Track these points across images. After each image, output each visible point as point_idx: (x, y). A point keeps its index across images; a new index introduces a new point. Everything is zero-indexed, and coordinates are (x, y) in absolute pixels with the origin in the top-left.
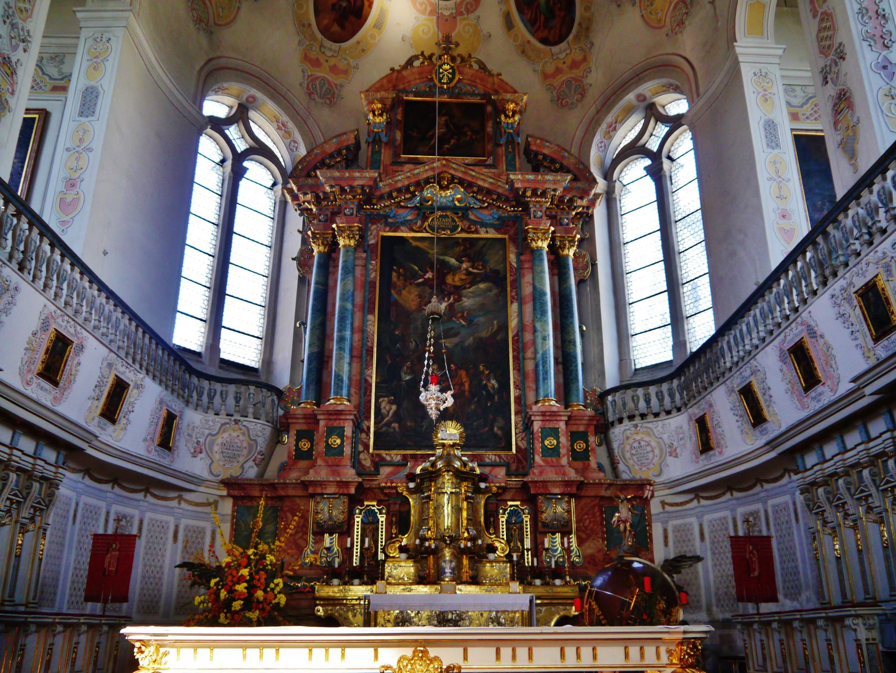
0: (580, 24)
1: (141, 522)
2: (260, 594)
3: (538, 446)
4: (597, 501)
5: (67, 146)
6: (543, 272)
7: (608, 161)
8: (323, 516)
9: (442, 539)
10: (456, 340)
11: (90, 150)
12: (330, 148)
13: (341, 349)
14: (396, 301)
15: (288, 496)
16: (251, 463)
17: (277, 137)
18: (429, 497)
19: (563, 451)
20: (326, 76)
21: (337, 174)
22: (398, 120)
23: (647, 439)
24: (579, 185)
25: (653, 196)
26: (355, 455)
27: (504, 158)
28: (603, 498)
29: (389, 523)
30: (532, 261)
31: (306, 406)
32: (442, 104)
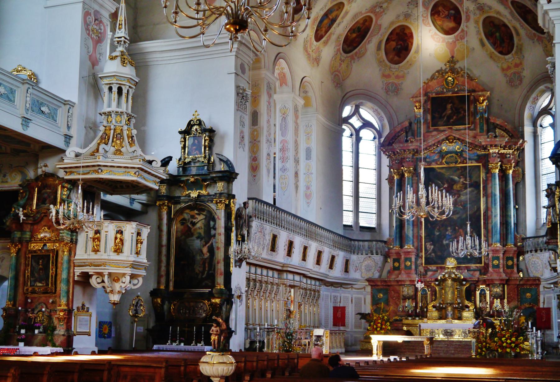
0: (517, 46)
1: (340, 297)
2: (384, 326)
3: (491, 264)
4: (516, 286)
5: (304, 172)
6: (495, 184)
8: (405, 293)
9: (448, 304)
10: (458, 216)
11: (312, 174)
12: (398, 129)
13: (408, 224)
15: (392, 285)
16: (376, 271)
17: (374, 115)
18: (442, 288)
19: (501, 266)
20: (394, 81)
21: (401, 145)
22: (428, 109)
23: (537, 260)
27: (479, 126)
28: (518, 285)
30: (492, 177)
31: (397, 248)
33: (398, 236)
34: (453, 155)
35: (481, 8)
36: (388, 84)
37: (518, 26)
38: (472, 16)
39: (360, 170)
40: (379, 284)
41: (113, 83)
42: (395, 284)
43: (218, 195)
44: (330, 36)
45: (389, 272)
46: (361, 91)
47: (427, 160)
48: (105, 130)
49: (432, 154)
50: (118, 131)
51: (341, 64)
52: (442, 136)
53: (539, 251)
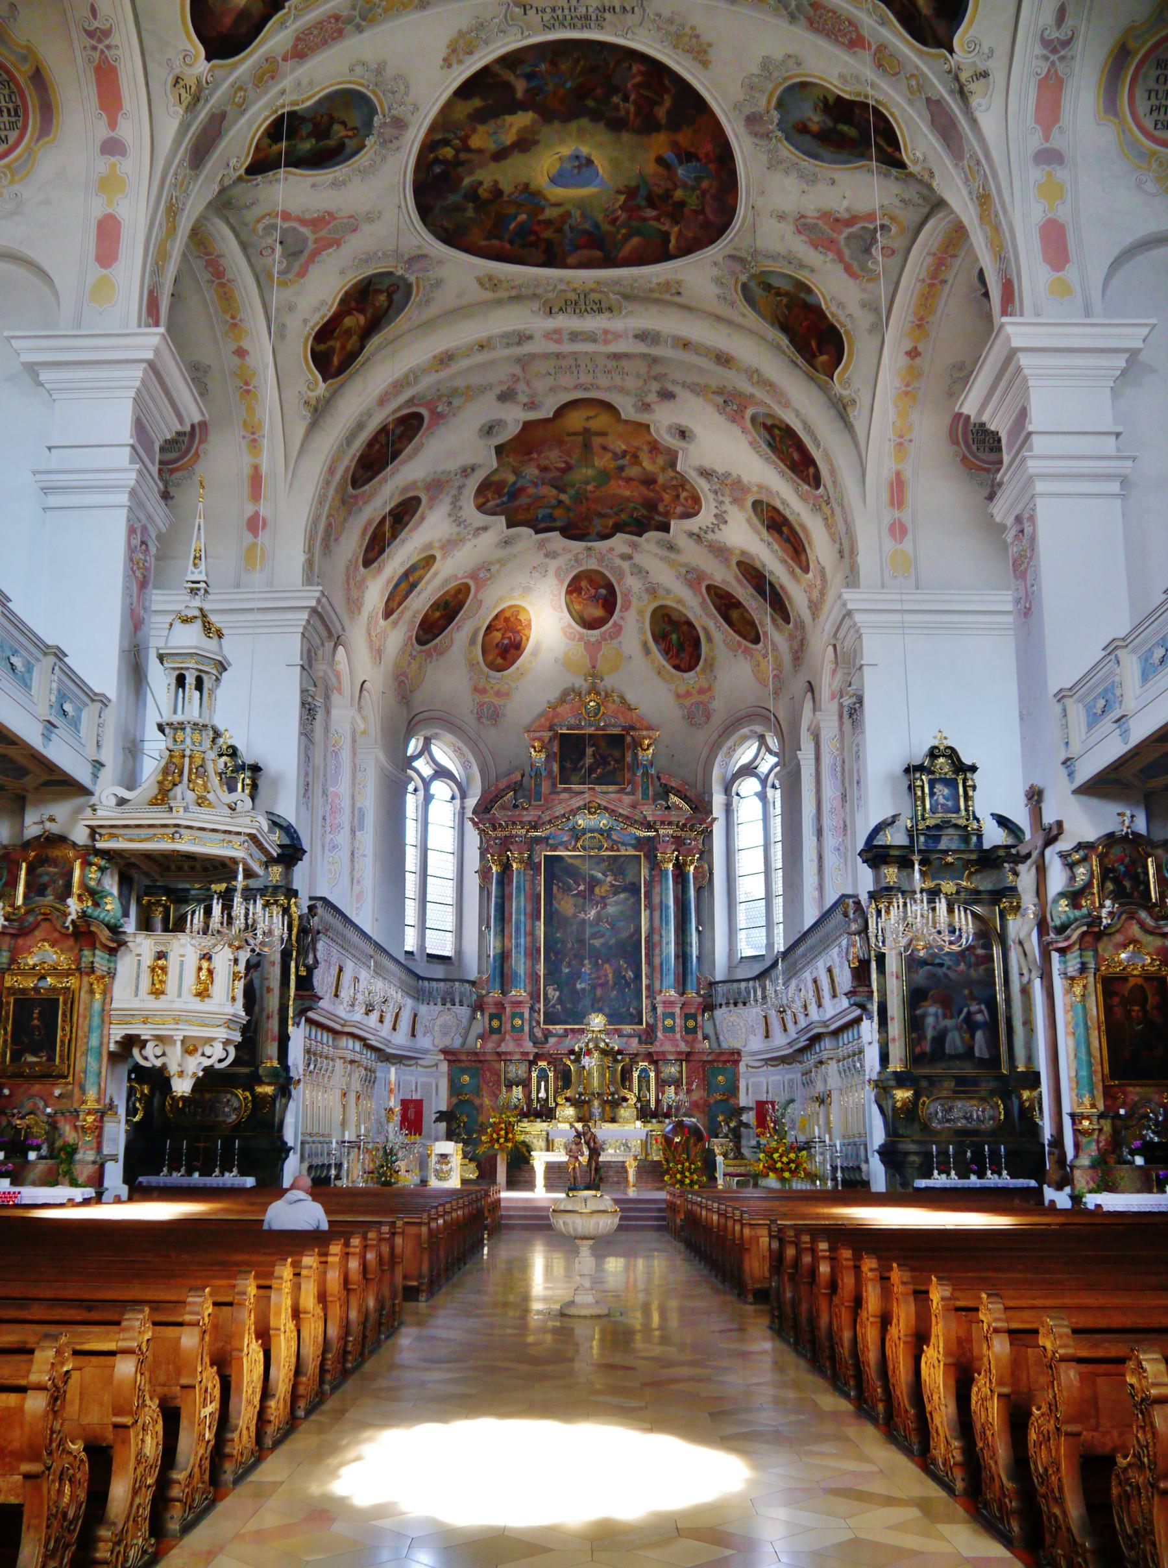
3: (660, 1025)
6: (667, 889)
7: (729, 775)
8: (511, 1076)
9: (593, 1094)
10: (602, 940)
11: (365, 856)
12: (503, 784)
13: (517, 952)
14: (557, 911)
19: (677, 1029)
24: (699, 816)
25: (761, 817)
26: (531, 1029)
29: (556, 1078)
31: (496, 994)
32: (590, 735)
33: (497, 971)
34: (596, 835)
35: (652, 591)
36: (481, 705)
37: (711, 625)
38: (634, 600)
39: (429, 852)
40: (464, 1057)
41: (188, 668)
42: (495, 1058)
43: (270, 890)
44: (402, 612)
45: (481, 1037)
46: (436, 714)
47: (551, 841)
48: (171, 756)
49: (560, 832)
50: (198, 762)
51: (410, 663)
52: (577, 802)
53: (740, 1005)
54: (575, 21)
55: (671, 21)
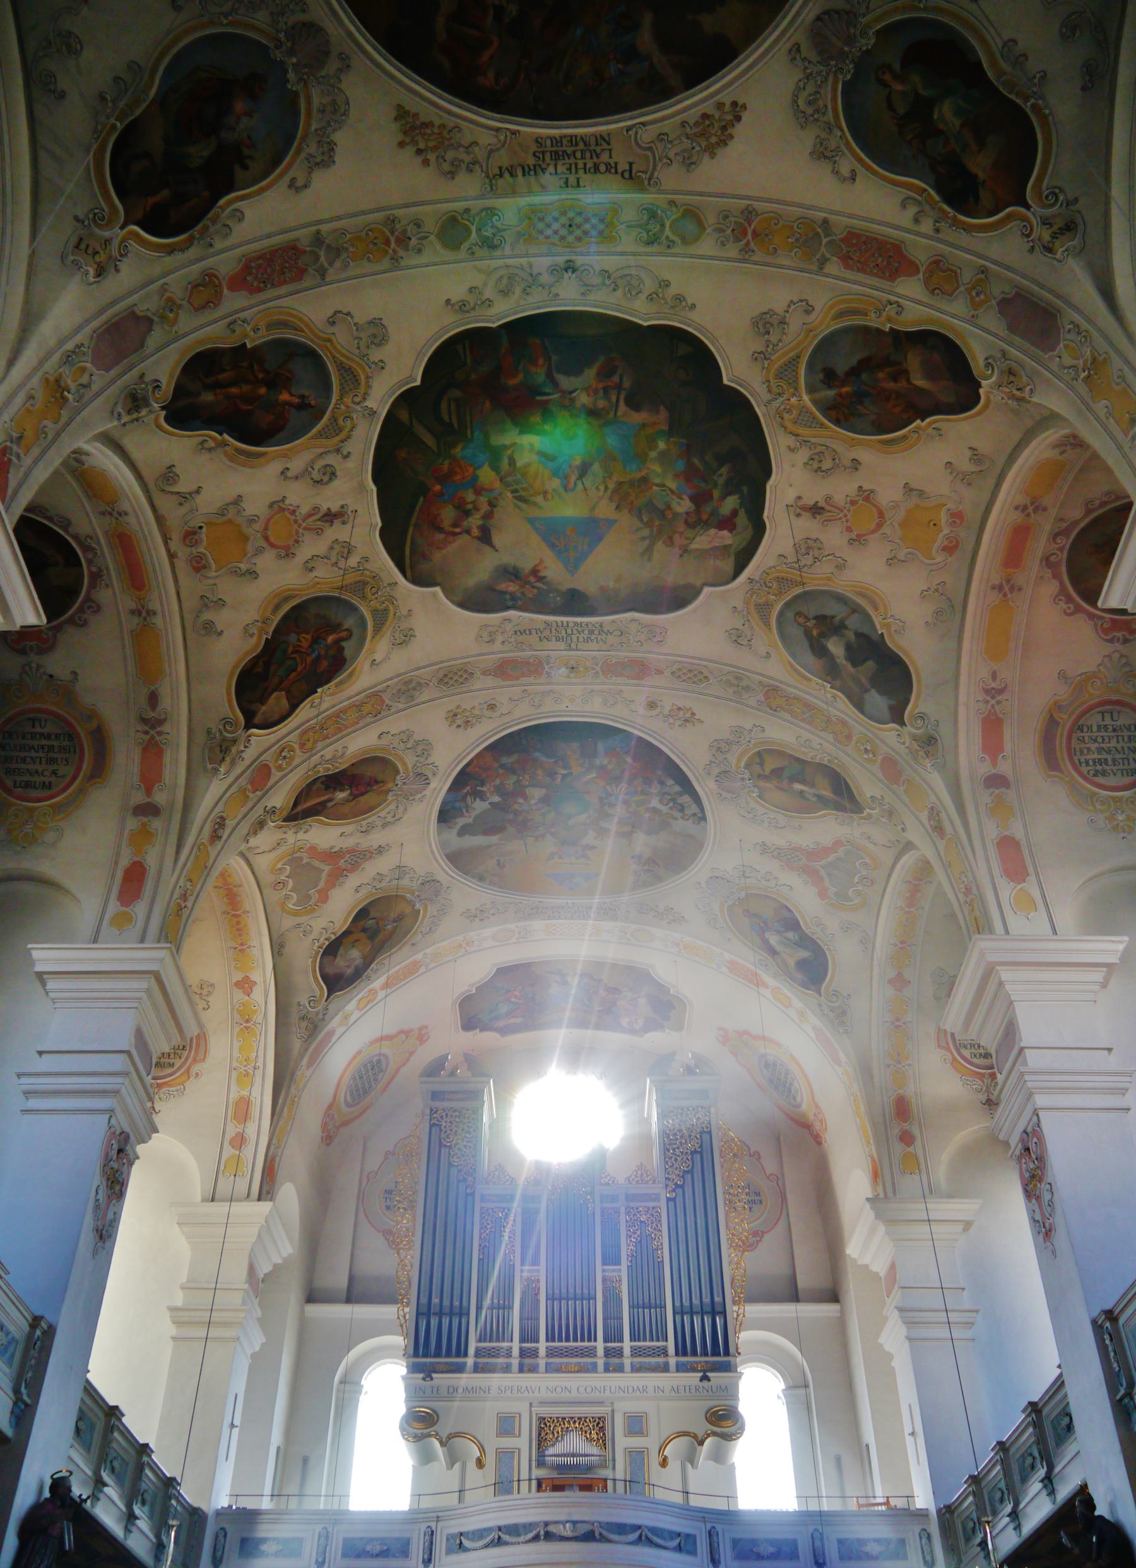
54: (569, 150)
55: (456, 164)
